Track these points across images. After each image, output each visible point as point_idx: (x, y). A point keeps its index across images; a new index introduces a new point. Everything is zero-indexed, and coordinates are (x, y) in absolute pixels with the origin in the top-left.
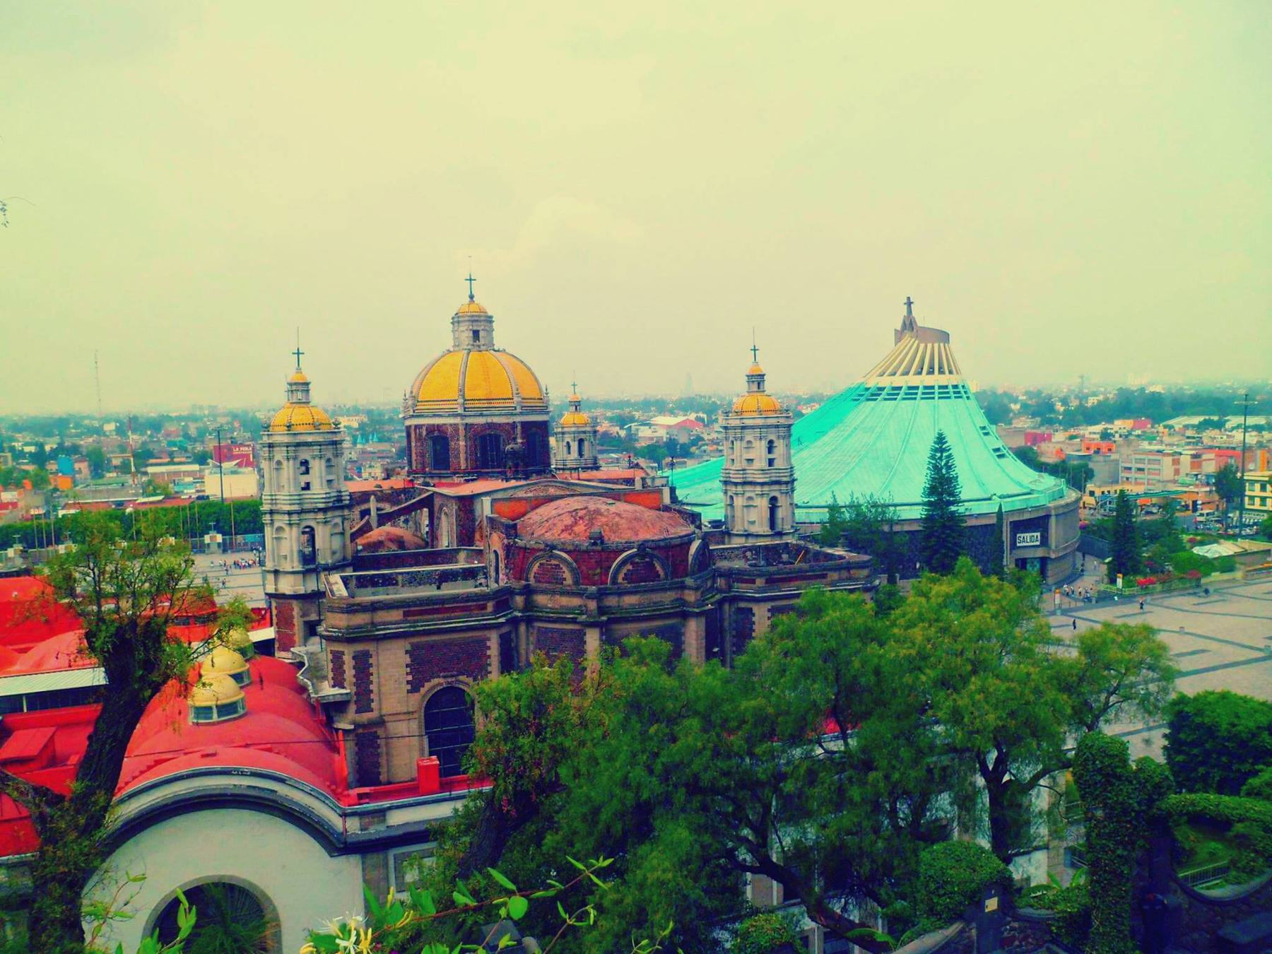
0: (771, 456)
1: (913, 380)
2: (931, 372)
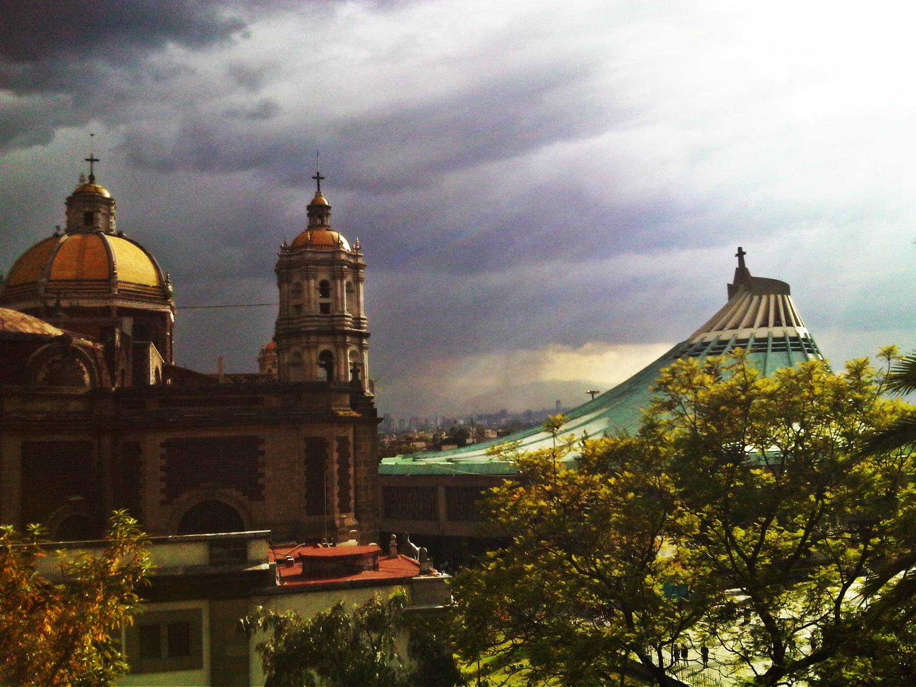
0: (325, 301)
1: (744, 334)
2: (765, 324)
